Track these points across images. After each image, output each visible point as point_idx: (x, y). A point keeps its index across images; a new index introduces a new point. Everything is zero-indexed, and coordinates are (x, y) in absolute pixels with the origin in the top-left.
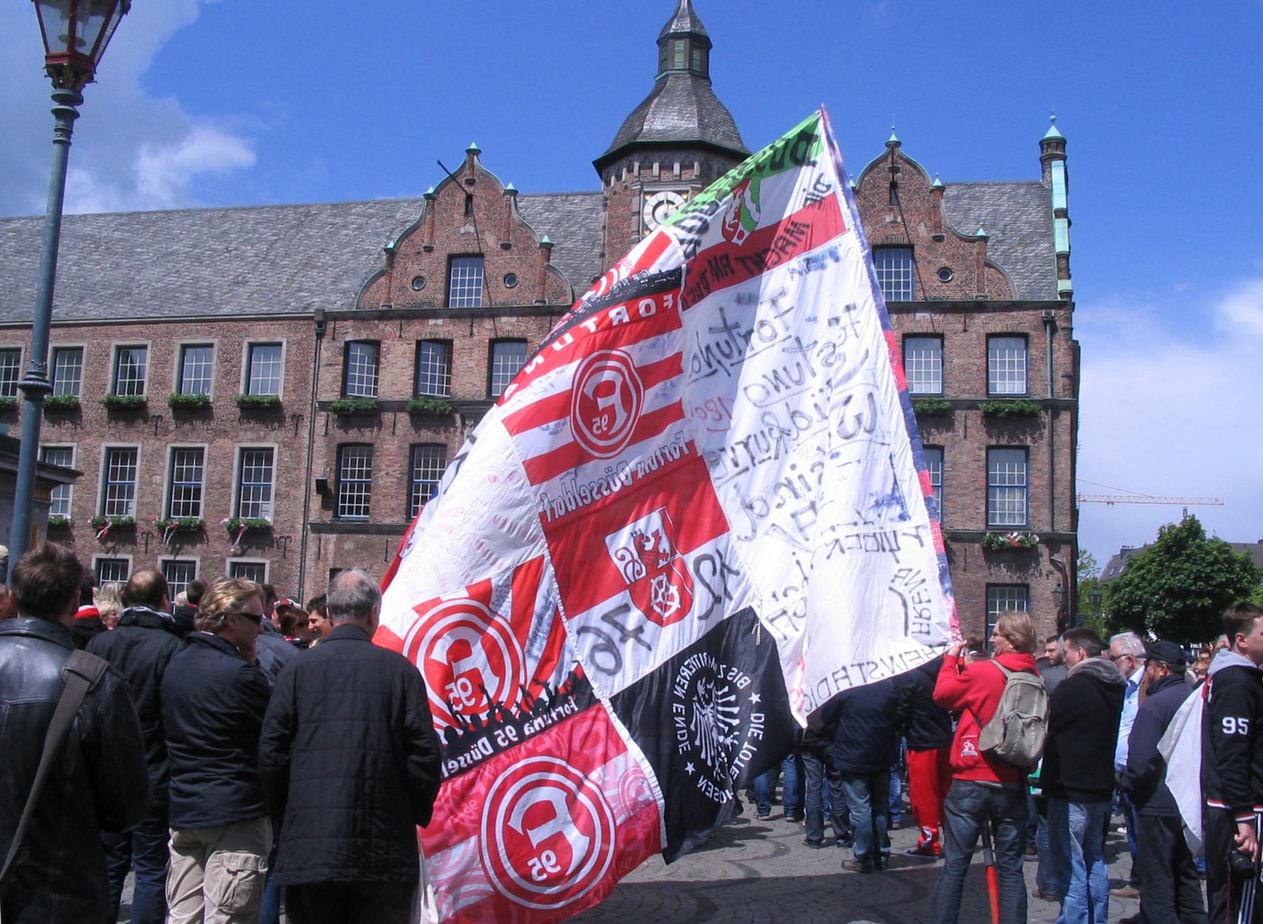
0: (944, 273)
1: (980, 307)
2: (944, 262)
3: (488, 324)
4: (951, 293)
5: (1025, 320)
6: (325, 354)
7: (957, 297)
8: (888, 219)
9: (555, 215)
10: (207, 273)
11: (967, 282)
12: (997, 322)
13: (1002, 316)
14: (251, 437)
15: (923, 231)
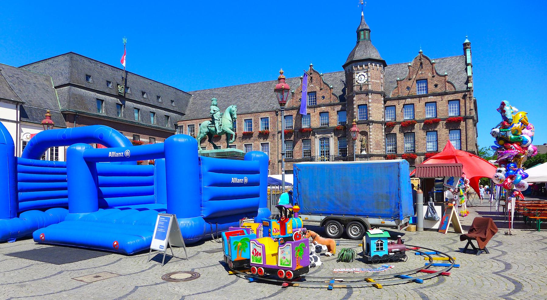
0: (436, 86)
1: (446, 94)
2: (436, 82)
3: (318, 109)
4: (438, 90)
5: (459, 96)
6: (279, 119)
7: (440, 91)
8: (420, 72)
9: (332, 79)
10: (247, 101)
11: (442, 87)
12: (451, 97)
13: (452, 95)
14: (262, 141)
15: (430, 75)
